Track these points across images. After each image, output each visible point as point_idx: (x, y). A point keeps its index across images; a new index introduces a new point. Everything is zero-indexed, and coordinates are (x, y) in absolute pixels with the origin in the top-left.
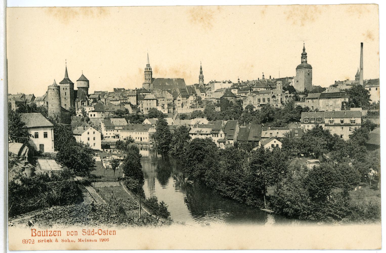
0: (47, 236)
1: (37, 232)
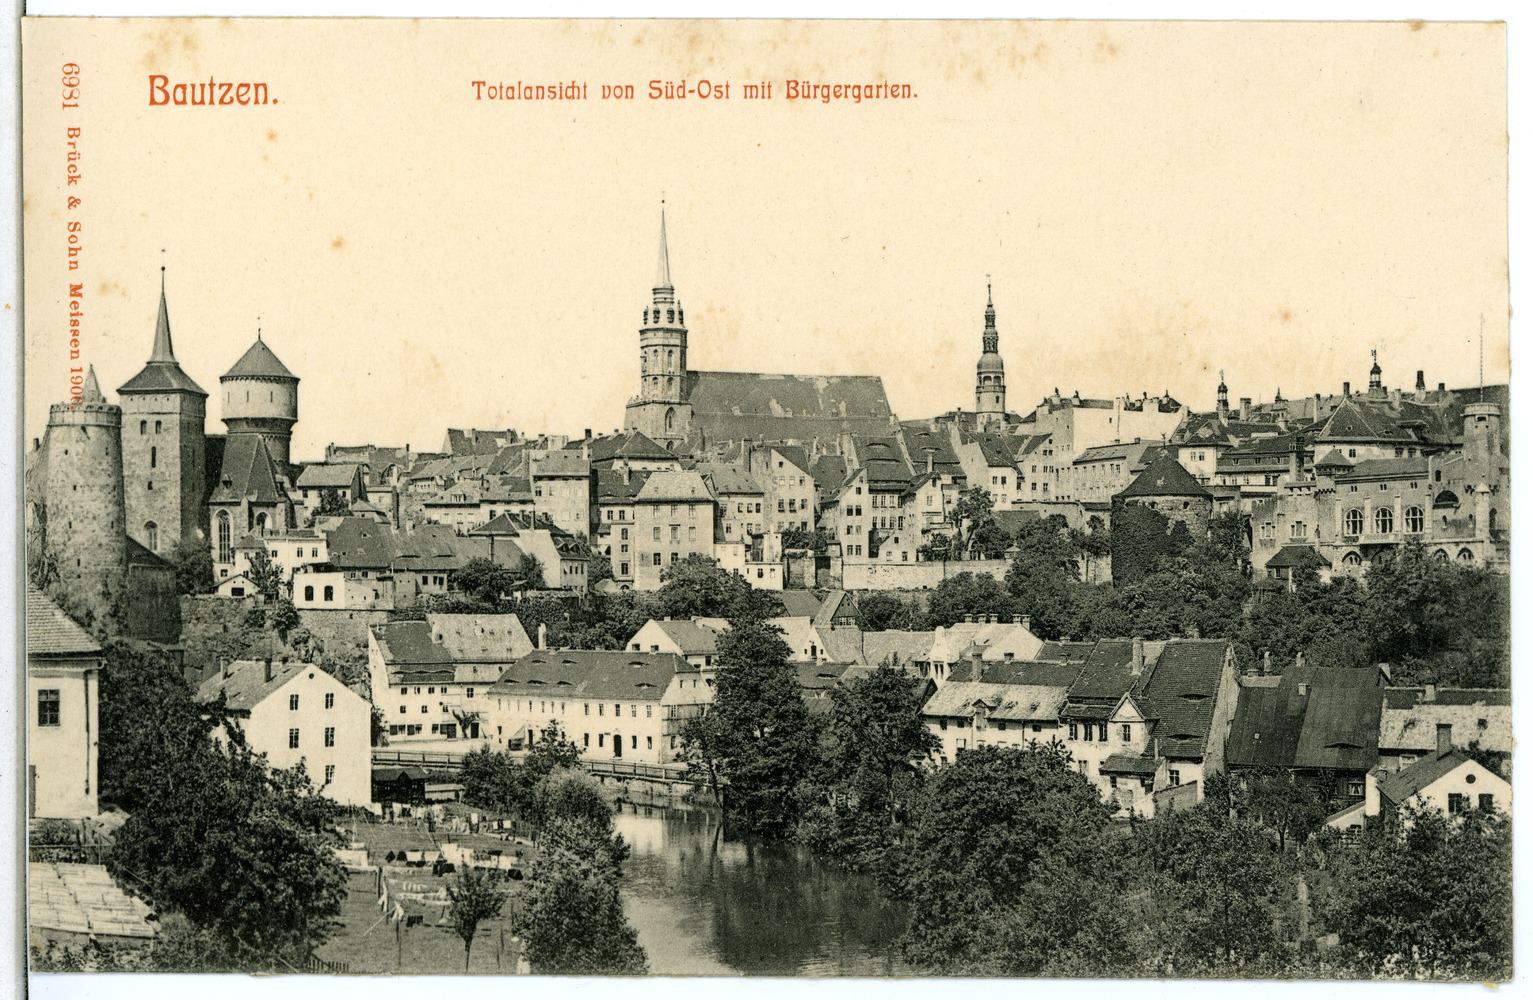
0: (212, 102)
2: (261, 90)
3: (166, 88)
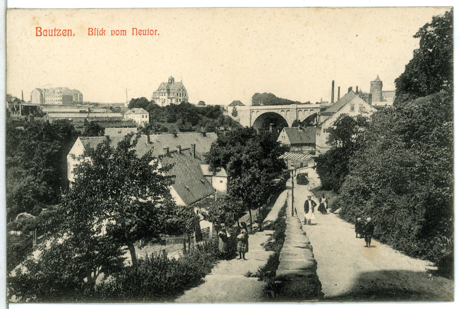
0: (55, 35)
1: (42, 31)
2: (70, 31)
3: (41, 31)
